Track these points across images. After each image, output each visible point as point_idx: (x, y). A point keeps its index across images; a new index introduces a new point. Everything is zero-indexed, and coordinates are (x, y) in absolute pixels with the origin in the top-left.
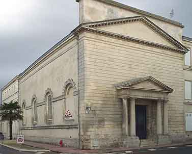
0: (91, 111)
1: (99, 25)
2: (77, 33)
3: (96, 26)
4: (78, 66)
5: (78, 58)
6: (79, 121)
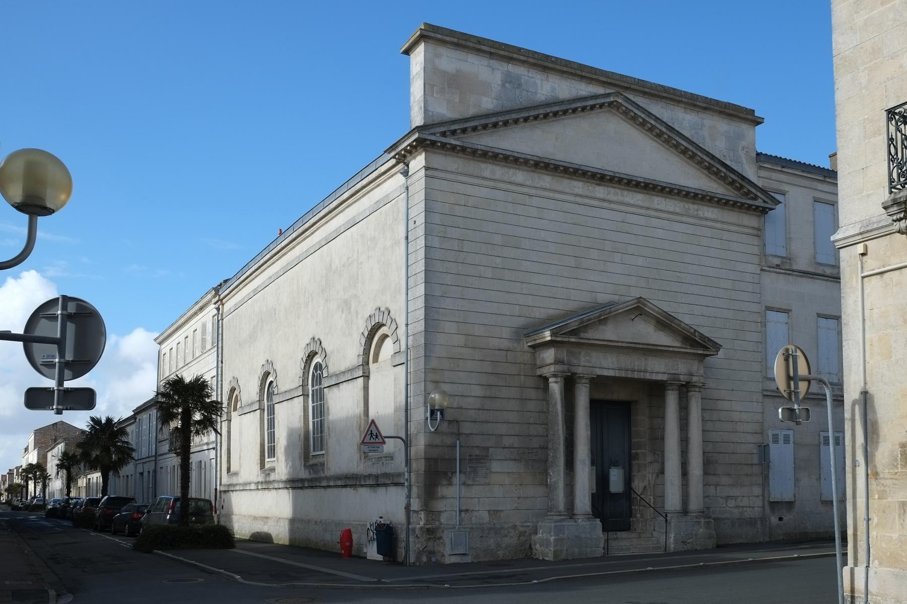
0: (445, 424)
1: (475, 129)
2: (405, 156)
3: (464, 131)
4: (408, 266)
5: (407, 238)
6: (408, 462)
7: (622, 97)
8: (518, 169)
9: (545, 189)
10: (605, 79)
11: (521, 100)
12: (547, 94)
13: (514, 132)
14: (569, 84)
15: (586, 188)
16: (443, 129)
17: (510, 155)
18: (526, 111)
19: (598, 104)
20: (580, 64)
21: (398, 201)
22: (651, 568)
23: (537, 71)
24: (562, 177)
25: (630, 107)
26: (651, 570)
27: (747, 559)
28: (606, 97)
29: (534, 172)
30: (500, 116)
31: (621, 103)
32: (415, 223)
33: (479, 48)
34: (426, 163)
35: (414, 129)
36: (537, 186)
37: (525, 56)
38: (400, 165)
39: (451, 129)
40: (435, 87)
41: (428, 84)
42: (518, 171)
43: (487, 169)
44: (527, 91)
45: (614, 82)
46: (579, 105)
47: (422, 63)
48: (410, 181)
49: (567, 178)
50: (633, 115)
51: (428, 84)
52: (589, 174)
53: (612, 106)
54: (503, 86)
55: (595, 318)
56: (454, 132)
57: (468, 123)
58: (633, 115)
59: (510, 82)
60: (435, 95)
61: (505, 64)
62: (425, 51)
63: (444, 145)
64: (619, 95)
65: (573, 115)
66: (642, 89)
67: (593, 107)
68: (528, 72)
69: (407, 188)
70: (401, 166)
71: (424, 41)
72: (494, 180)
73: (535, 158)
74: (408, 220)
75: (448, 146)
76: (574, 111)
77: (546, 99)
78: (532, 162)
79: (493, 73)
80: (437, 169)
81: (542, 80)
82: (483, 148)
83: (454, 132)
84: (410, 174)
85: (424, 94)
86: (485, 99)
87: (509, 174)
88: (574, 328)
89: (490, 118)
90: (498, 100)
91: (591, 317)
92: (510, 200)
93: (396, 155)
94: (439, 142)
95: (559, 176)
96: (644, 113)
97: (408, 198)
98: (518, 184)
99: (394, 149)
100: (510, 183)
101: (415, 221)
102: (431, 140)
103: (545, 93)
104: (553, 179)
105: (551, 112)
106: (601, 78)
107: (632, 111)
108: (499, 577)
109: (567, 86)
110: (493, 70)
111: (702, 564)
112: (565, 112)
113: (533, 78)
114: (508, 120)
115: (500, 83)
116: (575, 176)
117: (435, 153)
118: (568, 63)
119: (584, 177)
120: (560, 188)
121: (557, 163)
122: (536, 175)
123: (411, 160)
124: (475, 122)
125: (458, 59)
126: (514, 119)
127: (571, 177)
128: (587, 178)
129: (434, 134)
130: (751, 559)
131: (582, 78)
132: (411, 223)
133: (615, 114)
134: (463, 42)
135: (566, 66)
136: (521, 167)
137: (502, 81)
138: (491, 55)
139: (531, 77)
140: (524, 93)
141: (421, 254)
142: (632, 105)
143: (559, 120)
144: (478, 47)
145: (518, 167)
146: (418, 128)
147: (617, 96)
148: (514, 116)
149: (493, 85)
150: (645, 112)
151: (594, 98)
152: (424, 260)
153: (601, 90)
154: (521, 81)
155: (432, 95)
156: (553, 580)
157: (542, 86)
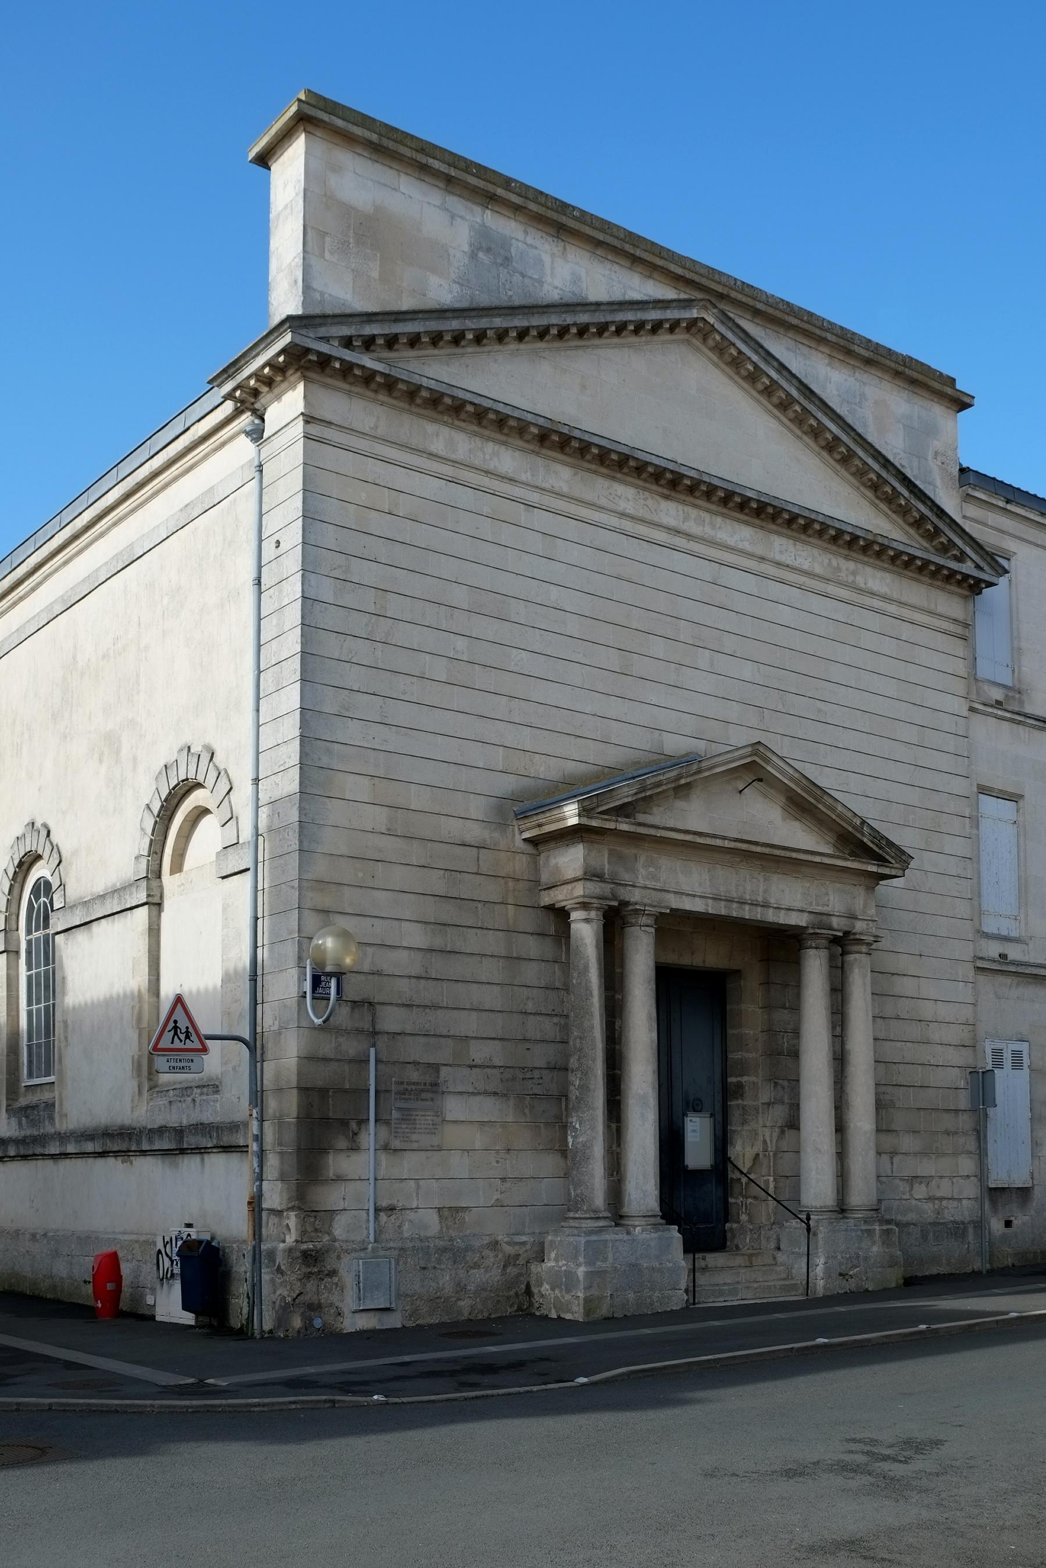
0: (345, 1010)
1: (414, 341)
2: (256, 393)
3: (391, 342)
4: (259, 646)
5: (258, 582)
6: (257, 1096)
7: (715, 311)
8: (504, 443)
9: (560, 495)
10: (679, 271)
11: (510, 293)
12: (564, 289)
13: (496, 361)
14: (607, 272)
15: (643, 502)
16: (346, 331)
17: (490, 409)
18: (523, 314)
19: (667, 320)
20: (631, 233)
21: (235, 501)
22: (826, 1340)
23: (544, 235)
24: (595, 472)
25: (730, 335)
26: (825, 1345)
27: (1007, 1313)
28: (684, 308)
29: (537, 454)
30: (470, 317)
31: (713, 326)
32: (277, 547)
33: (424, 161)
34: (305, 407)
35: (282, 323)
36: (544, 485)
37: (519, 195)
38: (244, 416)
39: (362, 333)
40: (328, 239)
41: (313, 228)
42: (503, 448)
43: (437, 435)
44: (523, 276)
45: (696, 278)
46: (630, 316)
47: (299, 181)
48: (266, 450)
49: (604, 476)
50: (735, 353)
51: (313, 228)
52: (650, 469)
53: (694, 330)
54: (473, 256)
55: (669, 781)
56: (369, 343)
57: (401, 324)
58: (735, 353)
59: (489, 250)
60: (327, 256)
61: (478, 209)
62: (307, 153)
63: (347, 370)
64: (708, 305)
65: (616, 340)
66: (750, 302)
67: (656, 327)
68: (526, 233)
69: (260, 468)
70: (246, 420)
71: (305, 130)
72: (455, 462)
73: (541, 421)
74: (260, 541)
75: (357, 372)
76: (621, 329)
77: (561, 299)
78: (534, 430)
79: (452, 224)
80: (330, 423)
81: (553, 255)
82: (432, 384)
83: (369, 343)
84: (265, 436)
85: (304, 251)
86: (434, 280)
87: (484, 453)
88: (626, 800)
89: (446, 318)
90: (462, 285)
91: (661, 778)
92: (486, 510)
93: (235, 390)
94: (337, 359)
95: (589, 470)
96: (757, 352)
97: (261, 489)
98: (503, 477)
99: (231, 377)
100: (487, 472)
101: (278, 542)
102: (319, 354)
103: (560, 285)
104: (576, 474)
105: (575, 324)
106: (673, 267)
107: (734, 345)
108: (488, 1368)
109: (604, 276)
110: (453, 217)
111: (923, 1327)
112: (602, 329)
113: (536, 248)
114: (485, 330)
115: (466, 248)
116: (620, 472)
117: (326, 386)
118: (607, 227)
119: (639, 477)
120: (589, 496)
121: (587, 437)
122: (540, 462)
123: (271, 402)
124: (416, 323)
125: (379, 183)
126: (498, 328)
127: (612, 473)
128: (645, 481)
129: (326, 339)
130: (1015, 1314)
131: (635, 261)
132: (268, 547)
133: (698, 350)
134: (391, 145)
135: (602, 230)
136: (510, 440)
137: (471, 245)
138: (449, 183)
139: (531, 246)
140: (516, 278)
141: (294, 615)
142: (733, 332)
143: (588, 347)
144: (423, 159)
145: (503, 438)
146: (291, 321)
147: (705, 308)
148: (498, 322)
149: (452, 252)
150: (760, 350)
151: (660, 305)
152: (298, 630)
153: (669, 293)
154: (510, 252)
155: (322, 256)
156: (623, 1374)
157: (553, 269)
